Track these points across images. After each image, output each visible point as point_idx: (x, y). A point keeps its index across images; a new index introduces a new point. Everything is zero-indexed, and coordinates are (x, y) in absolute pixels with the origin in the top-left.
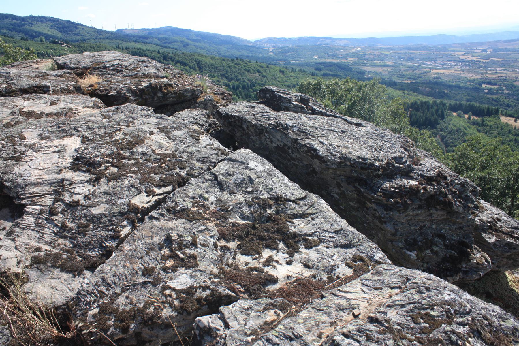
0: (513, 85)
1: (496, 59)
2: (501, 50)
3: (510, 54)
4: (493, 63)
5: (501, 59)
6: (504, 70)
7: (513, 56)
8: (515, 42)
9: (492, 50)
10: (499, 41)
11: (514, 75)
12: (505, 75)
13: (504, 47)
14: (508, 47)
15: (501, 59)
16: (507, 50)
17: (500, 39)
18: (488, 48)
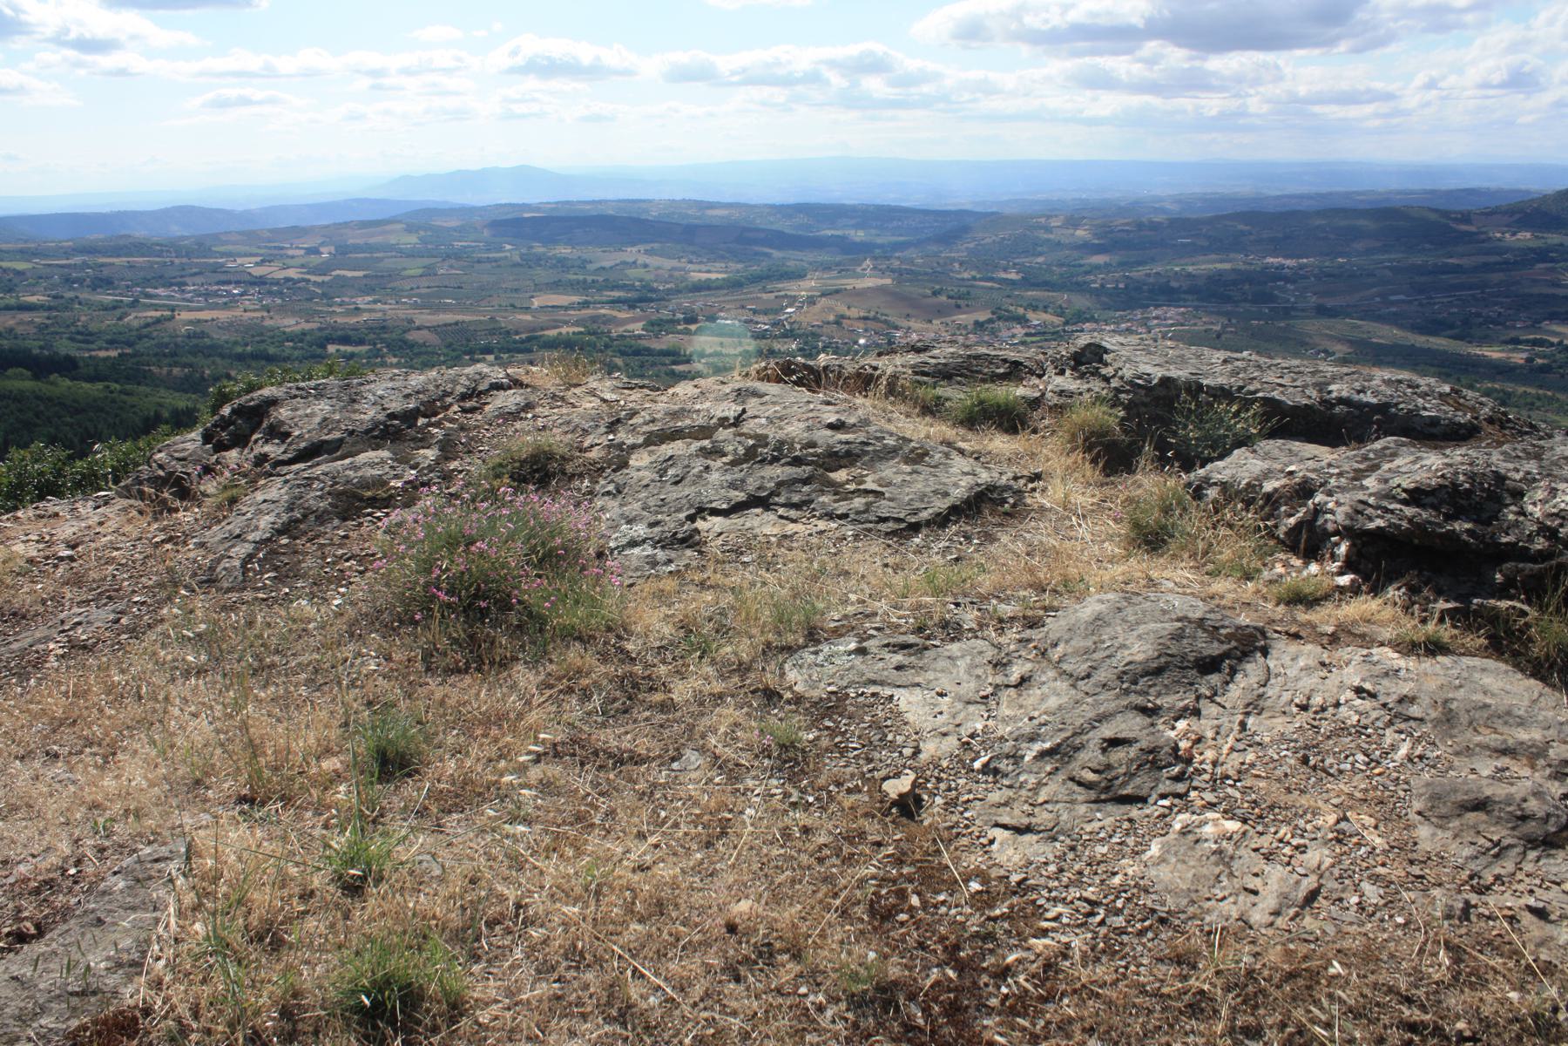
0: (405, 342)
1: (350, 274)
2: (357, 248)
3: (381, 260)
4: (343, 283)
5: (360, 274)
6: (375, 302)
7: (389, 263)
8: (388, 228)
9: (332, 249)
10: (346, 224)
11: (402, 314)
12: (379, 315)
13: (360, 241)
14: (372, 241)
15: (360, 274)
16: (370, 248)
17: (348, 219)
18: (322, 244)
